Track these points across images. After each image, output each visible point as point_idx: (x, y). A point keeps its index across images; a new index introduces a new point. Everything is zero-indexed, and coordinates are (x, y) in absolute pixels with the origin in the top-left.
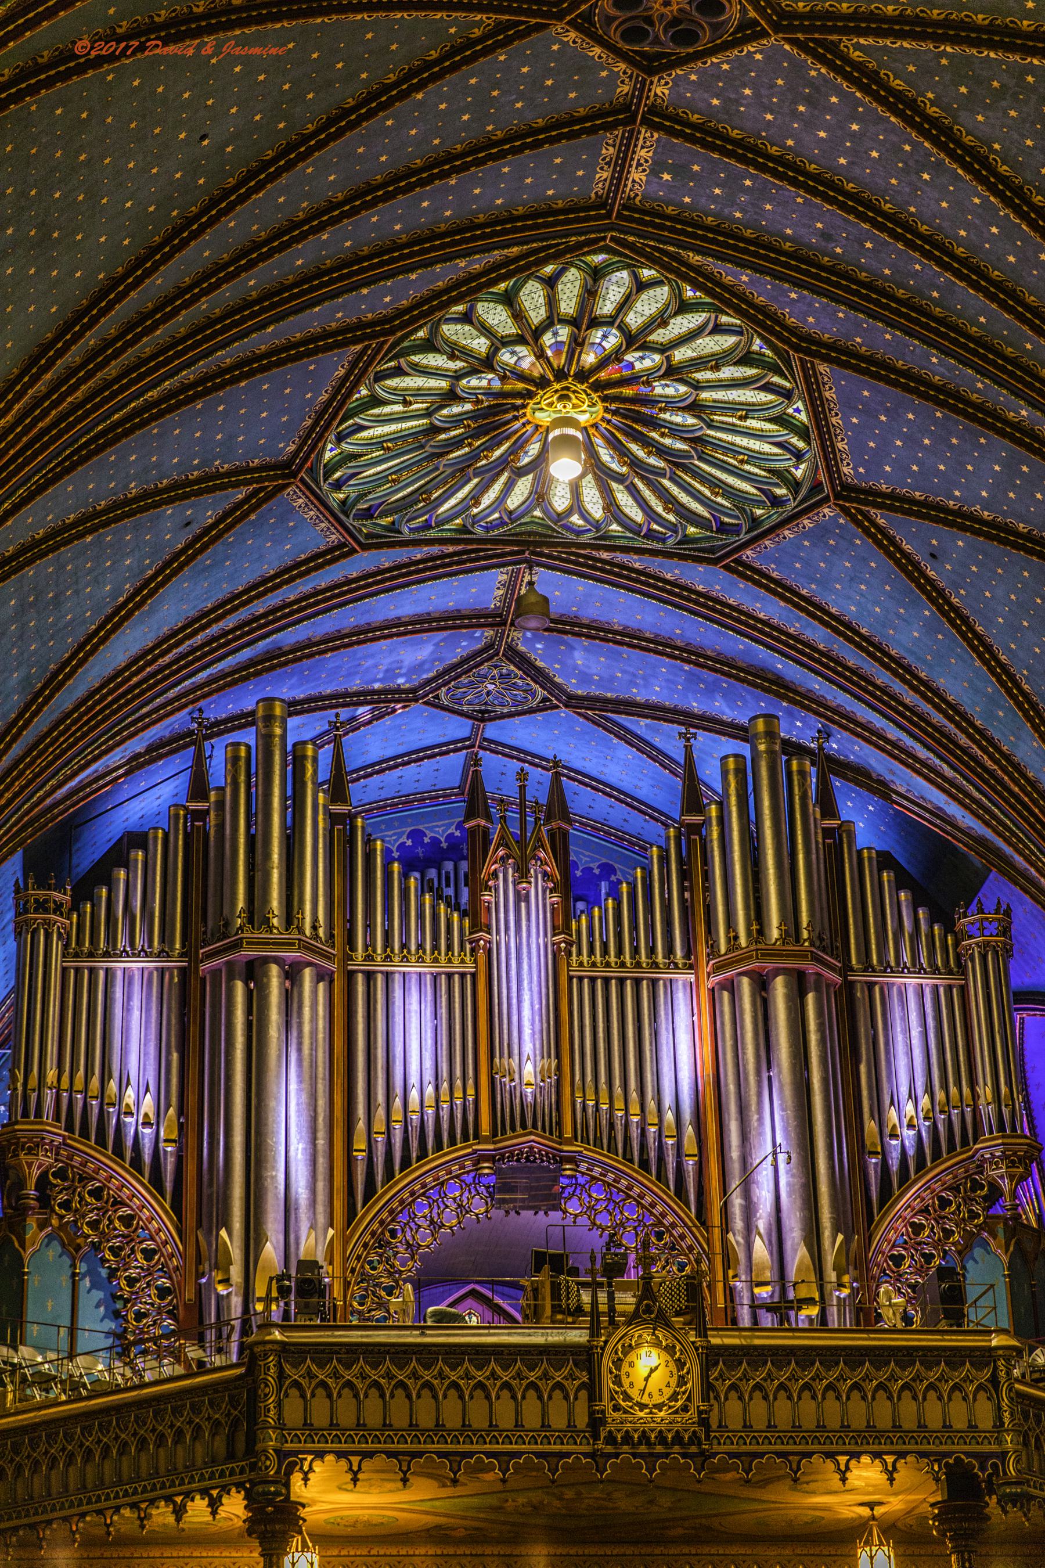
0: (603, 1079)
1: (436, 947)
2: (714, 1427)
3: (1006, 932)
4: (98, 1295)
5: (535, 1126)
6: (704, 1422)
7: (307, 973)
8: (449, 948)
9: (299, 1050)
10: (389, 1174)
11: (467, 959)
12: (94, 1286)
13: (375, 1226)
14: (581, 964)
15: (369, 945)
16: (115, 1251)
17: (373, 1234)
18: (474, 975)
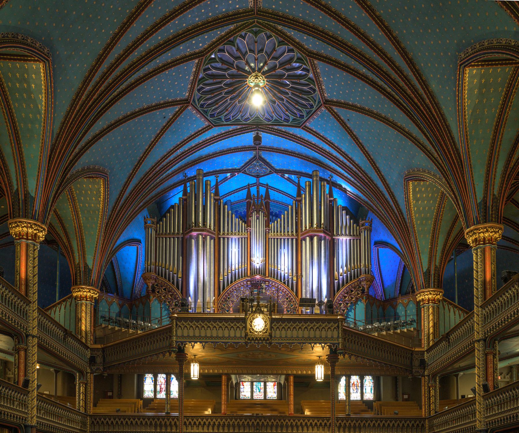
0: (276, 262)
1: (239, 231)
2: (273, 336)
3: (371, 226)
4: (166, 312)
5: (259, 273)
6: (270, 335)
7: (208, 237)
8: (242, 231)
9: (206, 256)
10: (228, 284)
11: (246, 234)
12: (165, 310)
13: (224, 297)
14: (272, 235)
15: (224, 230)
16: (169, 302)
17: (224, 298)
18: (247, 238)
